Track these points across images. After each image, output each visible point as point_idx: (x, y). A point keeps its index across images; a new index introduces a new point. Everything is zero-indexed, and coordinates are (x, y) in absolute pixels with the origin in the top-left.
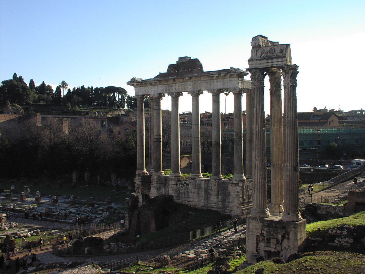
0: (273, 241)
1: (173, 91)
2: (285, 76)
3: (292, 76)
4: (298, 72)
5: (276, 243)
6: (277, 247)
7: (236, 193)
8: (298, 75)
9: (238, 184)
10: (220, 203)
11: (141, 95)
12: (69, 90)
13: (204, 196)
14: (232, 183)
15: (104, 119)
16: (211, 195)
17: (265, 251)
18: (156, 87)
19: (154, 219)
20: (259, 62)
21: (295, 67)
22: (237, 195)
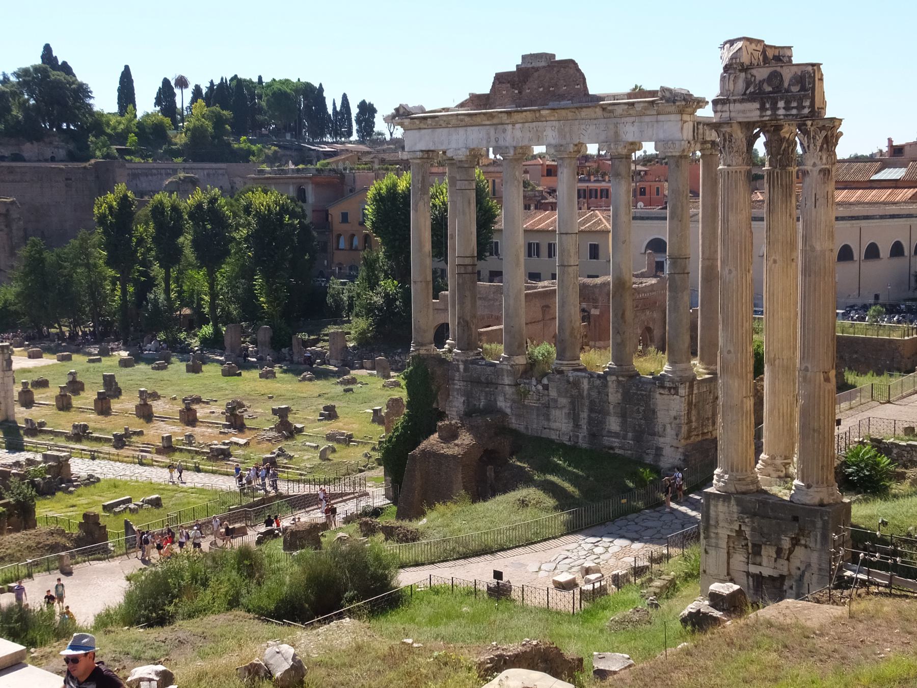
0: (768, 552)
1: (507, 144)
2: (806, 145)
3: (825, 146)
4: (841, 134)
5: (775, 556)
6: (778, 566)
7: (673, 413)
8: (841, 140)
9: (676, 389)
10: (630, 435)
11: (422, 151)
12: (197, 91)
13: (589, 416)
14: (663, 387)
15: (302, 180)
16: (608, 414)
17: (748, 574)
18: (461, 131)
19: (460, 476)
20: (739, 106)
21: (835, 123)
22: (675, 418)
